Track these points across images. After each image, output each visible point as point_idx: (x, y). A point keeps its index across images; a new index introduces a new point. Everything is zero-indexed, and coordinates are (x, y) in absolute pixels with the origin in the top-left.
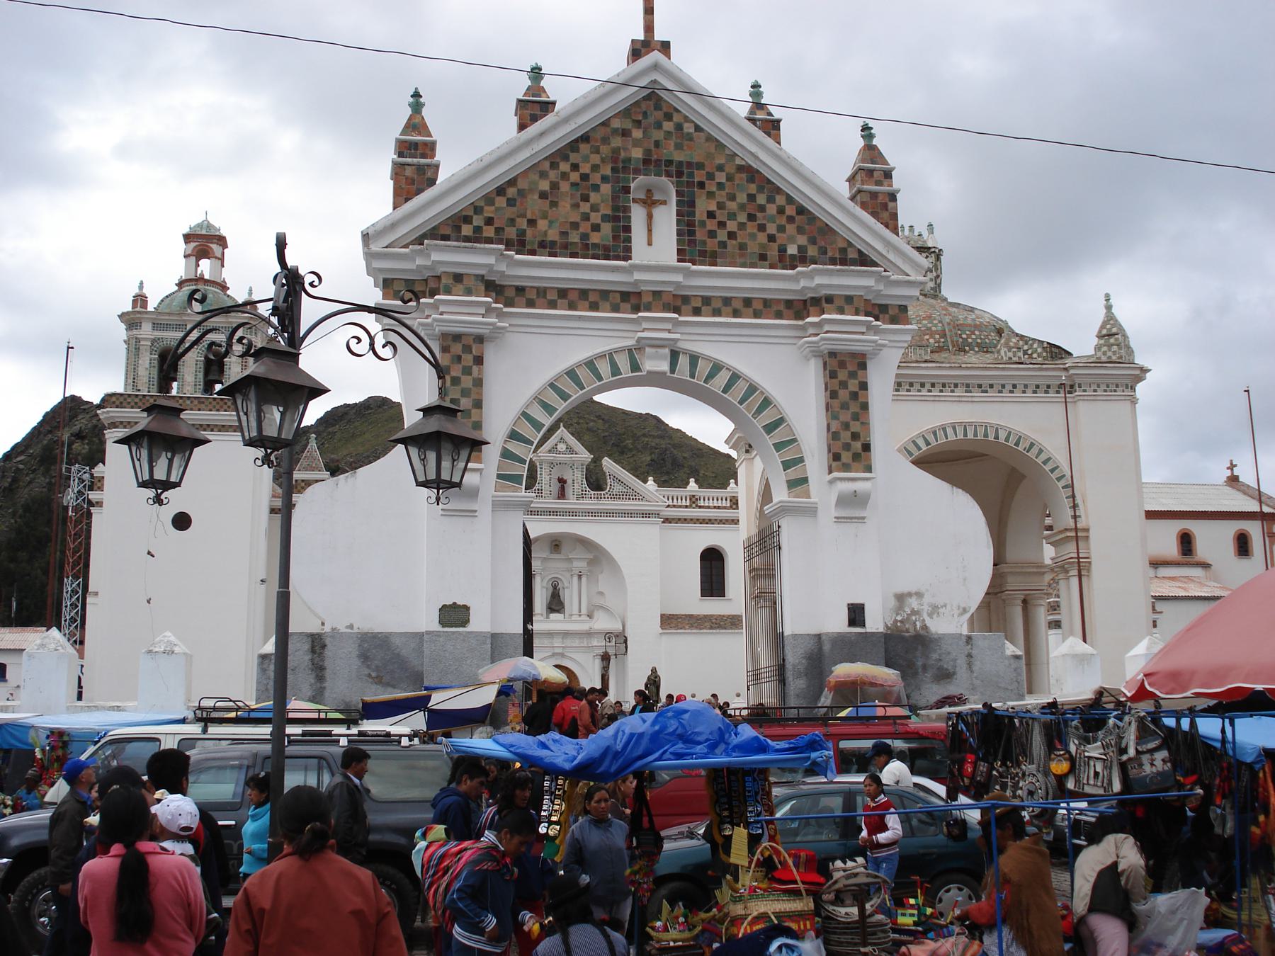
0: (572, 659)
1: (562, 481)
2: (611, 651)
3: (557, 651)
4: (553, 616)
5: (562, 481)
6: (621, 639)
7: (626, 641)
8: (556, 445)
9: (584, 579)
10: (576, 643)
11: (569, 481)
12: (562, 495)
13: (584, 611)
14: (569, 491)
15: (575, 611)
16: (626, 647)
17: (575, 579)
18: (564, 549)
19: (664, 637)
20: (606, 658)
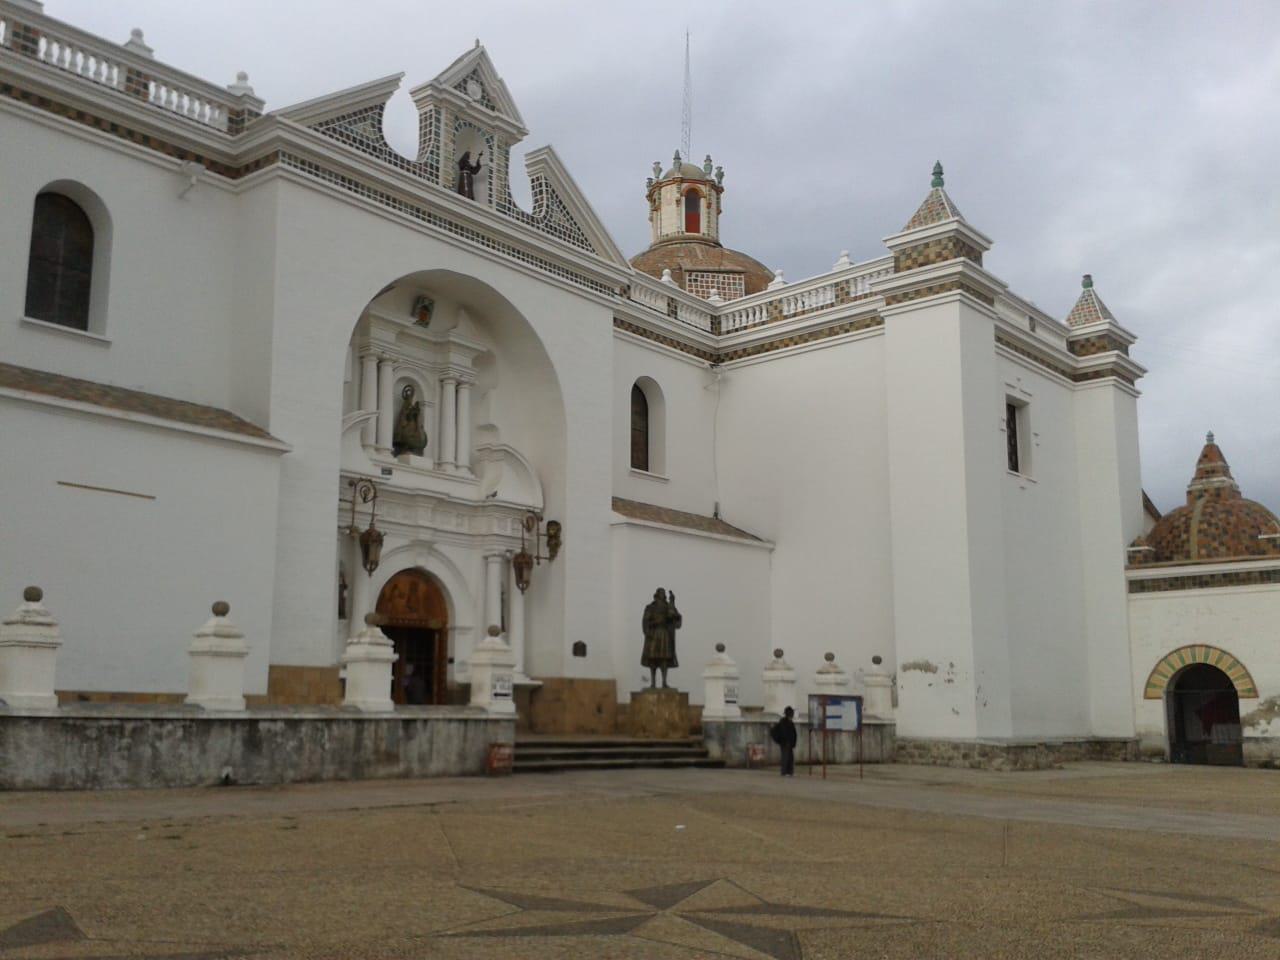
0: (448, 563)
3: (425, 536)
4: (413, 459)
8: (465, 81)
9: (465, 393)
10: (450, 523)
13: (464, 459)
14: (481, 188)
17: (450, 389)
18: (439, 318)
19: (626, 531)
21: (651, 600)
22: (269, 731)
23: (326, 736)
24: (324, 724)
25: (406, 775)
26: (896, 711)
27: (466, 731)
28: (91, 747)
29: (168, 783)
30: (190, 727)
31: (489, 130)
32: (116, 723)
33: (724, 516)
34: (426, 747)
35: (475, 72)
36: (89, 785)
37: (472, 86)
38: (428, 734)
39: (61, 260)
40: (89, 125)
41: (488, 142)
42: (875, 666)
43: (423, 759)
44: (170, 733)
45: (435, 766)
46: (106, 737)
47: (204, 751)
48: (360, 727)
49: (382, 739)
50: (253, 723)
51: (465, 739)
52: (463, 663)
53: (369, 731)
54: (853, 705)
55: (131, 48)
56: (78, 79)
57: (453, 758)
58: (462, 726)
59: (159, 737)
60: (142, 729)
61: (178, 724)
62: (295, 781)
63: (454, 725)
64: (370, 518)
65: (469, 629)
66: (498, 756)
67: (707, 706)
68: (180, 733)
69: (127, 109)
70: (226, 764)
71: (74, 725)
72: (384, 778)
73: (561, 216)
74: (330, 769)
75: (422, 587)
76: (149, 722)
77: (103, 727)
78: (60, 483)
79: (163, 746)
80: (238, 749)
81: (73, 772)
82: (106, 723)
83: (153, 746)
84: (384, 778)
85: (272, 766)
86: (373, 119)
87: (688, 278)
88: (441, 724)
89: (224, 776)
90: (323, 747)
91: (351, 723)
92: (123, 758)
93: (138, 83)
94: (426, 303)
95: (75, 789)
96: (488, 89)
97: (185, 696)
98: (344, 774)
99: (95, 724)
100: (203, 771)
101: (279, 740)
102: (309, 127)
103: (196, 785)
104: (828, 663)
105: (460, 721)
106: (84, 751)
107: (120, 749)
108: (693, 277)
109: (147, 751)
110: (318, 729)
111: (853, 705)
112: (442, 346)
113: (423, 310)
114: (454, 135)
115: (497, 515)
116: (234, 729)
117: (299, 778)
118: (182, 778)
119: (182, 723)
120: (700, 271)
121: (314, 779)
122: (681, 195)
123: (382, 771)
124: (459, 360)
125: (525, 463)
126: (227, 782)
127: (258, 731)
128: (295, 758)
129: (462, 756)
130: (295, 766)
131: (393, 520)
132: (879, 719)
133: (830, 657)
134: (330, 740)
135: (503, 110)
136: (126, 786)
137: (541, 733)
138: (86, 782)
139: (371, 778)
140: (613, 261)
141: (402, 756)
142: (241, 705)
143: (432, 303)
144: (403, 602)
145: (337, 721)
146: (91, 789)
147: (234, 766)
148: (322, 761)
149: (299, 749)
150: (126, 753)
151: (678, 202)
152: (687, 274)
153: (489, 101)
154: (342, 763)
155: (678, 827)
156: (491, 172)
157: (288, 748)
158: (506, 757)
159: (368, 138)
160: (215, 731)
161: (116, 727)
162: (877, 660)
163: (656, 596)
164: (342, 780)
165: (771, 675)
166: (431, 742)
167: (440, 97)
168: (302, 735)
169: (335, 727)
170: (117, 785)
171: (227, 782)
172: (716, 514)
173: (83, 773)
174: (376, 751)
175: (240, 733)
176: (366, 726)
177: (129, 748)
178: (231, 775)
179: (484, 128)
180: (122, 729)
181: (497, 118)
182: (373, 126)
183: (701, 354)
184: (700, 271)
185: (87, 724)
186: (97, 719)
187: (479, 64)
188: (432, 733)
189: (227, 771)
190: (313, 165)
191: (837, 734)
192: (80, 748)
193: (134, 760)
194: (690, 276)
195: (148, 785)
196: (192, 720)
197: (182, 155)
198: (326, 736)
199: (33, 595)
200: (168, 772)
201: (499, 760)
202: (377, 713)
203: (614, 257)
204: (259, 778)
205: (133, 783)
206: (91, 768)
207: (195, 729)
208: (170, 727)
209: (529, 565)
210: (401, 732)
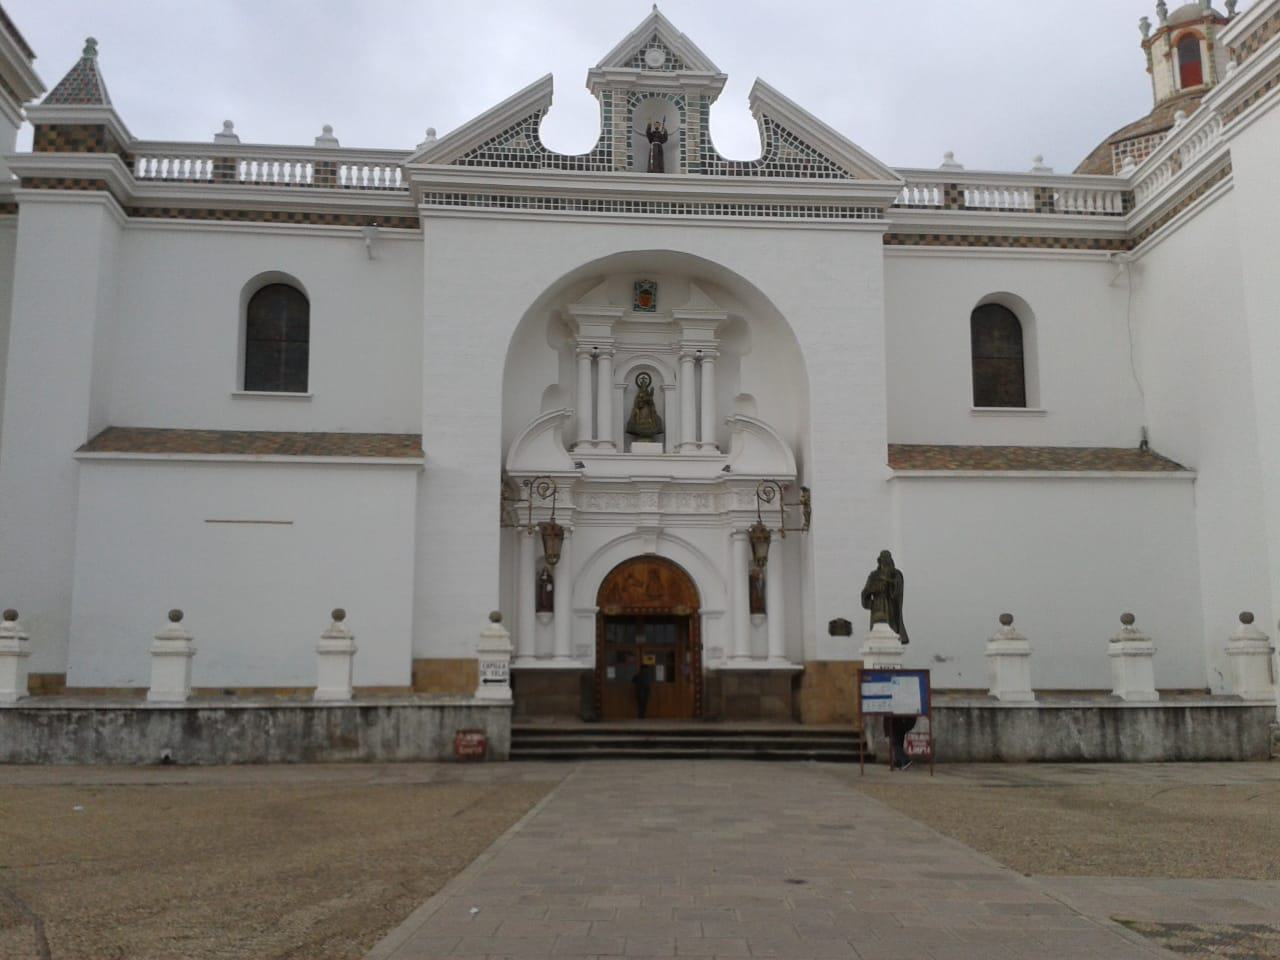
0: (686, 545)
1: (657, 137)
2: (772, 523)
3: (653, 522)
4: (639, 447)
5: (657, 137)
6: (795, 494)
7: (806, 504)
8: (643, 53)
10: (691, 506)
11: (674, 138)
12: (658, 164)
13: (708, 435)
14: (673, 156)
15: (689, 435)
16: (808, 515)
17: (688, 367)
18: (665, 299)
19: (898, 487)
20: (758, 538)
21: (875, 566)
22: (209, 718)
23: (271, 722)
24: (268, 712)
25: (368, 759)
26: (1275, 688)
27: (442, 718)
28: (43, 731)
29: (109, 761)
30: (131, 715)
31: (678, 91)
32: (65, 712)
33: (1155, 445)
34: (391, 733)
35: (655, 38)
36: (40, 761)
37: (655, 57)
38: (393, 721)
39: (284, 338)
40: (284, 222)
41: (677, 103)
42: (1242, 626)
43: (387, 745)
44: (111, 721)
45: (403, 751)
46: (55, 723)
47: (143, 735)
48: (310, 714)
49: (335, 726)
50: (192, 712)
51: (441, 725)
52: (715, 649)
53: (319, 720)
54: (915, 681)
55: (321, 146)
56: (288, 188)
57: (427, 744)
58: (437, 714)
59: (102, 723)
60: (85, 717)
61: (119, 713)
62: (237, 763)
63: (426, 713)
64: (550, 512)
65: (721, 613)
66: (464, 743)
67: (320, 689)
68: (121, 720)
69: (326, 199)
70: (166, 746)
71: (29, 715)
72: (339, 762)
73: (792, 150)
74: (275, 754)
75: (664, 574)
76: (93, 711)
77: (53, 716)
78: (207, 521)
79: (106, 731)
80: (178, 734)
81: (28, 751)
82: (55, 713)
83: (97, 731)
84: (339, 762)
85: (213, 750)
86: (528, 129)
87: (1114, 152)
88: (409, 711)
89: (163, 756)
90: (267, 732)
91: (298, 711)
92: (70, 740)
93: (326, 172)
94: (646, 287)
95: (28, 763)
96: (673, 49)
97: (988, 690)
98: (294, 757)
99: (46, 713)
100: (143, 752)
101: (219, 726)
102: (454, 163)
103: (134, 764)
104: (1123, 627)
105: (434, 708)
106: (37, 735)
107: (67, 733)
108: (1121, 149)
109: (92, 735)
110: (261, 717)
111: (915, 681)
112: (675, 325)
113: (645, 296)
114: (630, 111)
115: (735, 490)
116: (173, 717)
117: (241, 760)
118: (123, 757)
119: (123, 712)
120: (1129, 139)
121: (258, 762)
122: (1171, 47)
123: (338, 755)
124: (697, 337)
125: (768, 429)
126: (166, 762)
127: (197, 718)
128: (237, 742)
129: (438, 742)
130: (237, 749)
131: (617, 511)
132: (1242, 700)
133: (1128, 619)
134: (275, 725)
135: (692, 65)
136: (73, 762)
137: (714, 719)
138: (39, 757)
139: (324, 762)
140: (876, 178)
141: (361, 742)
142: (1031, 696)
143: (654, 285)
144: (641, 590)
145: (284, 709)
146: (43, 764)
147: (173, 748)
148: (267, 745)
149: (241, 734)
150: (73, 737)
151: (1168, 56)
152: (1113, 147)
153: (676, 61)
154: (290, 749)
155: (76, 808)
156: (683, 133)
157: (229, 734)
158: (475, 743)
159: (522, 151)
160: (154, 719)
161: (64, 716)
162: (1247, 618)
163: (879, 560)
164: (290, 762)
165: (1118, 647)
166: (397, 729)
167: (603, 80)
168: (244, 722)
169: (280, 715)
170: (64, 761)
171: (166, 762)
172: (1145, 443)
173: (36, 751)
174: (330, 737)
175: (179, 720)
176: (316, 713)
177: (75, 733)
178: (170, 755)
179: (670, 92)
180: (69, 718)
181: (679, 77)
182: (528, 136)
183: (1097, 244)
184: (1129, 139)
185: (39, 713)
186: (48, 709)
187: (656, 29)
188: (398, 720)
189: (164, 753)
190: (459, 197)
191: (373, 713)
192: (34, 732)
193: (81, 744)
194: (1117, 148)
195: (93, 762)
196: (133, 710)
197: (369, 221)
198: (271, 722)
199: (176, 616)
200: (110, 752)
201: (466, 746)
202: (327, 701)
203: (873, 173)
204: (198, 759)
205: (79, 761)
206: (43, 747)
207: (135, 717)
208: (112, 715)
209: (767, 539)
210: (359, 719)
